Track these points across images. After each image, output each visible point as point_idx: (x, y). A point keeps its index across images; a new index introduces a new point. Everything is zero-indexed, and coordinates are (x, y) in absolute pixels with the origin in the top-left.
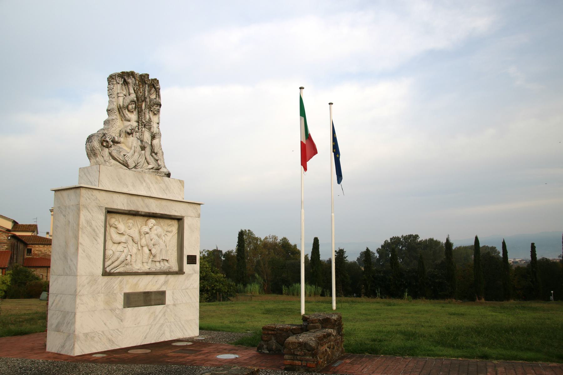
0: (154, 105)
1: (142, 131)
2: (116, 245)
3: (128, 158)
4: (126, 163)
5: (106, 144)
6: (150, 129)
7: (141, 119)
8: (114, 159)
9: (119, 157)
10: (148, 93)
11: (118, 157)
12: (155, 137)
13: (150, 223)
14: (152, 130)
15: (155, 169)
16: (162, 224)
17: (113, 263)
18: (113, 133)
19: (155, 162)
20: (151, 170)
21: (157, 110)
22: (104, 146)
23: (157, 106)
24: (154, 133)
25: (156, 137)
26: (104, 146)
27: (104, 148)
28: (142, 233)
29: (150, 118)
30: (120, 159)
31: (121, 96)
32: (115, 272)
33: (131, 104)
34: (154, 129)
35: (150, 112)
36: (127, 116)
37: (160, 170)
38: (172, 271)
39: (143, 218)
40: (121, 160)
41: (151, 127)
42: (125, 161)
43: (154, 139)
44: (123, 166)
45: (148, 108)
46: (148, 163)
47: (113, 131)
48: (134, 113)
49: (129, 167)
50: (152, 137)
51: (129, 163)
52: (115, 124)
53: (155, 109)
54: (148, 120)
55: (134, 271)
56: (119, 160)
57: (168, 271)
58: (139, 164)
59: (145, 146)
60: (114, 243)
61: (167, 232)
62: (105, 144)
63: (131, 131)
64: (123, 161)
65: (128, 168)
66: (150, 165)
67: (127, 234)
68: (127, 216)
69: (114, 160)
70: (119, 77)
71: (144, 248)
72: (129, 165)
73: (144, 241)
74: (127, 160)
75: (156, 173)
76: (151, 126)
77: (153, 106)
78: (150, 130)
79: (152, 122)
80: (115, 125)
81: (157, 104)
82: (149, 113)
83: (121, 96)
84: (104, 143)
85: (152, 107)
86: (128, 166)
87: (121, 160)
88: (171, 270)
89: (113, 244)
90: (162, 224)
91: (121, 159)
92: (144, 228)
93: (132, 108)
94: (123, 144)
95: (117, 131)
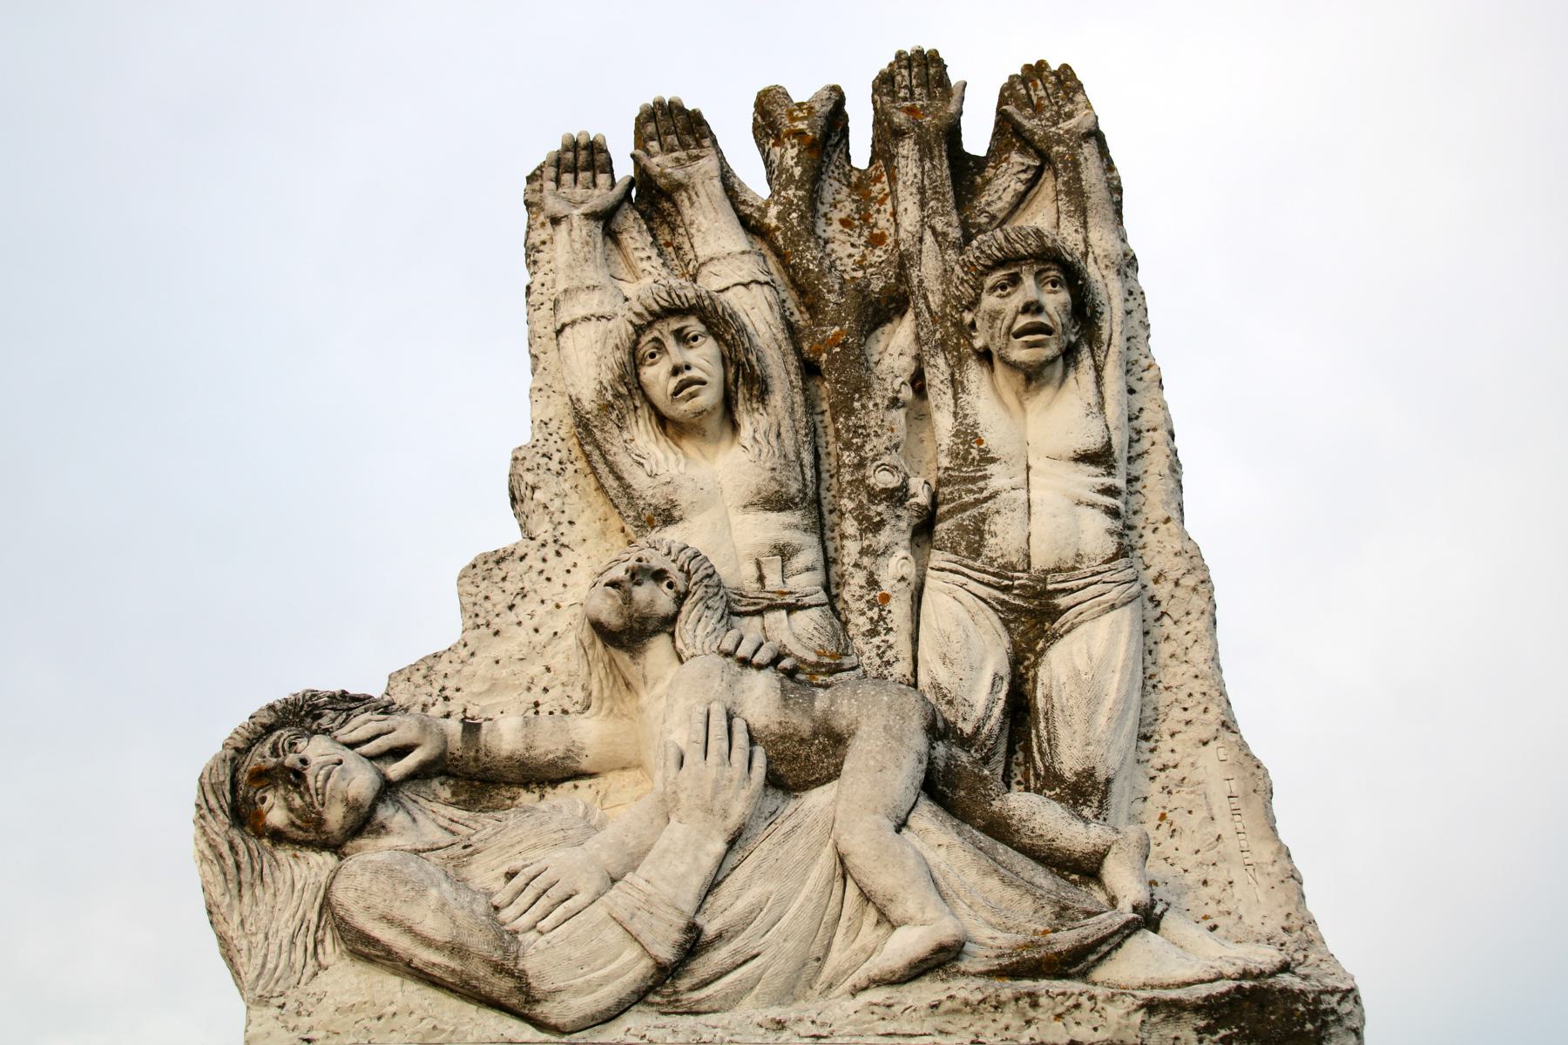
0: (978, 288)
1: (872, 583)
3: (544, 902)
4: (499, 969)
5: (291, 809)
6: (974, 540)
7: (861, 465)
8: (365, 949)
9: (399, 911)
10: (923, 205)
11: (390, 921)
12: (1059, 613)
14: (1004, 538)
15: (989, 974)
18: (493, 687)
19: (993, 883)
20: (927, 991)
21: (1023, 321)
22: (278, 837)
23: (1015, 280)
24: (1038, 563)
25: (1063, 601)
26: (278, 837)
27: (284, 854)
29: (968, 435)
30: (410, 930)
31: (573, 323)
33: (659, 343)
34: (1036, 527)
35: (974, 374)
36: (638, 480)
37: (1100, 974)
40: (428, 942)
41: (983, 518)
42: (480, 942)
43: (1055, 637)
44: (471, 1009)
45: (943, 345)
46: (886, 920)
47: (503, 673)
48: (746, 432)
49: (545, 1010)
50: (1009, 615)
51: (530, 964)
52: (523, 594)
53: (994, 316)
54: (953, 454)
56: (400, 943)
58: (718, 957)
59: (840, 724)
62: (277, 816)
63: (628, 599)
64: (456, 949)
65: (540, 1025)
66: (899, 931)
69: (369, 959)
70: (574, 169)
72: (539, 986)
74: (526, 920)
75: (1008, 1017)
76: (977, 502)
77: (974, 304)
78: (975, 550)
79: (991, 469)
80: (524, 608)
81: (999, 264)
82: (956, 385)
83: (573, 323)
84: (270, 796)
85: (968, 317)
86: (532, 1000)
87: (428, 942)
91: (432, 924)
93: (673, 383)
94: (628, 776)
95: (557, 663)
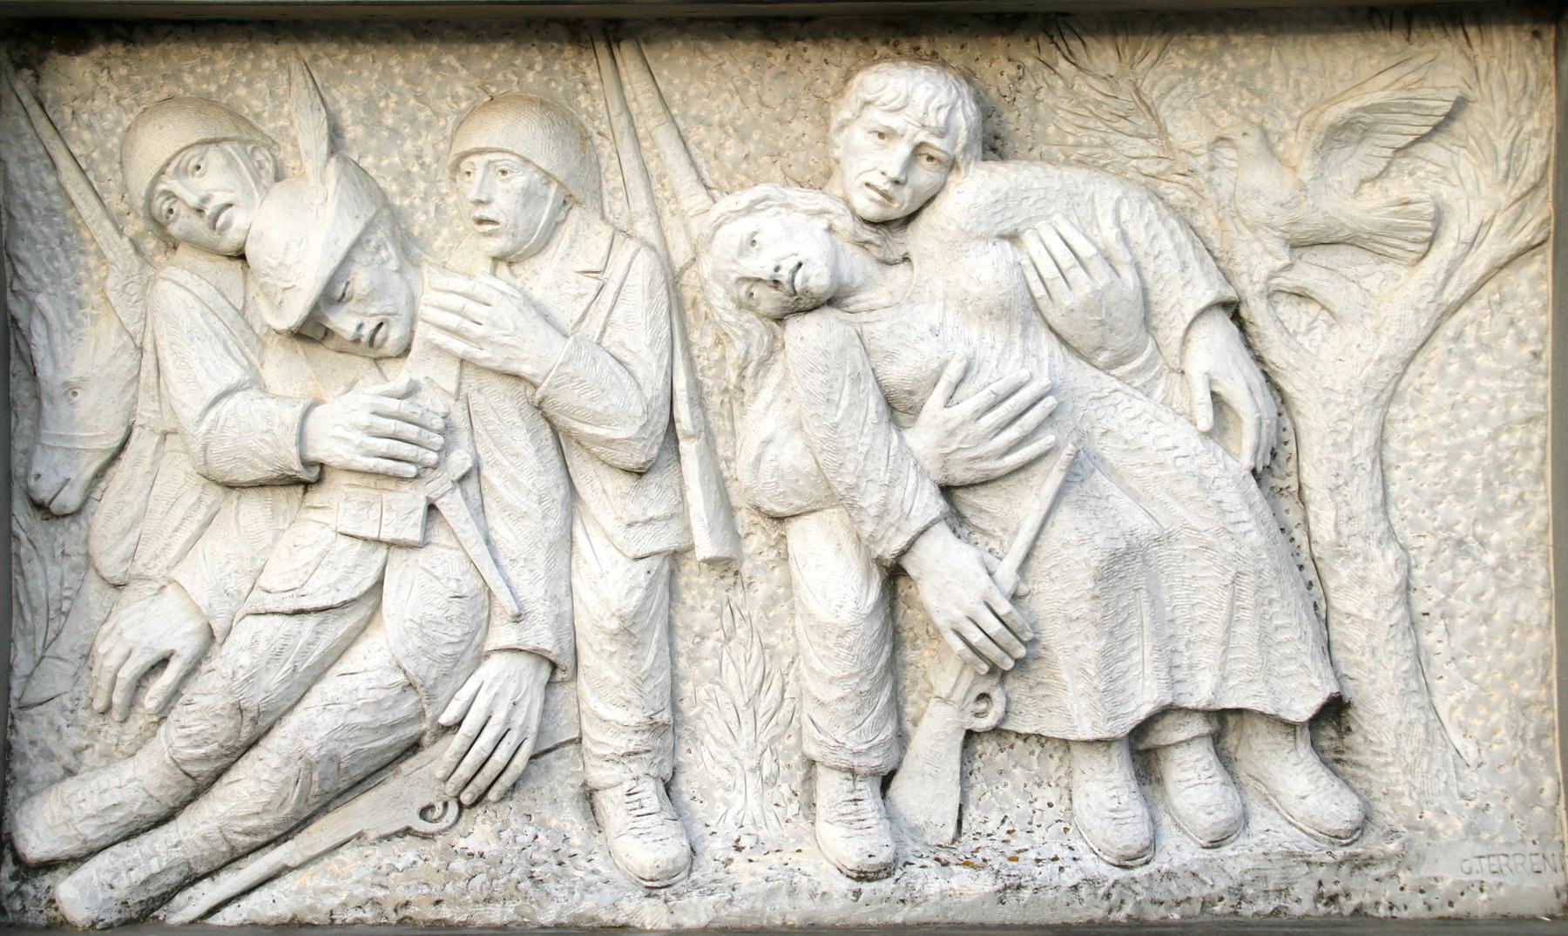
2: (253, 511)
13: (859, 136)
16: (1187, 130)
17: (199, 788)
28: (719, 299)
32: (229, 916)
38: (1416, 908)
39: (779, 55)
55: (548, 916)
57: (1302, 904)
60: (231, 486)
61: (1298, 245)
67: (438, 349)
68: (450, 59)
71: (794, 529)
73: (767, 427)
88: (1388, 892)
89: (214, 493)
90: (1187, 130)
92: (737, 231)
